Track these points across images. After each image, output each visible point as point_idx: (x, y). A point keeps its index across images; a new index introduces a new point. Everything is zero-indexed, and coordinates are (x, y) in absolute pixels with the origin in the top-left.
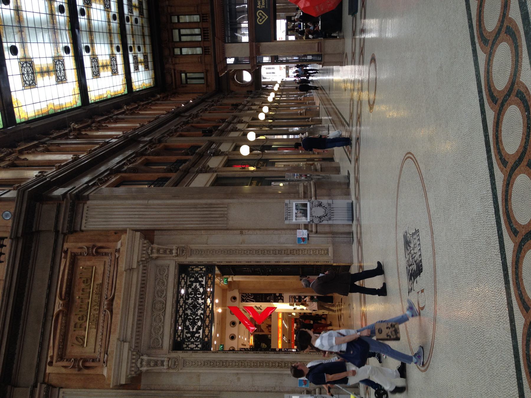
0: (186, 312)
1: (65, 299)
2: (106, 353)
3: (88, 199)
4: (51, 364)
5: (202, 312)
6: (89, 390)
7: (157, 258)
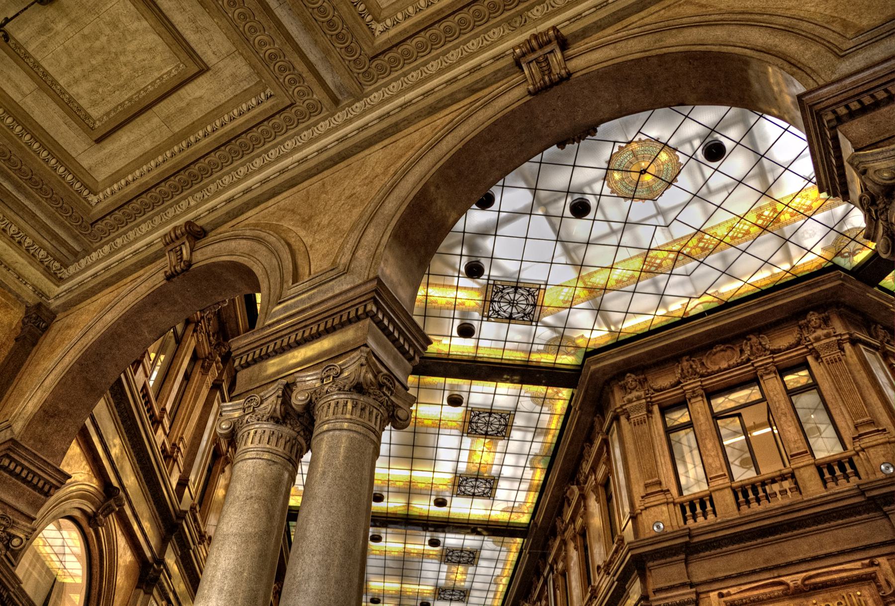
1: (805, 585)
4: (721, 595)
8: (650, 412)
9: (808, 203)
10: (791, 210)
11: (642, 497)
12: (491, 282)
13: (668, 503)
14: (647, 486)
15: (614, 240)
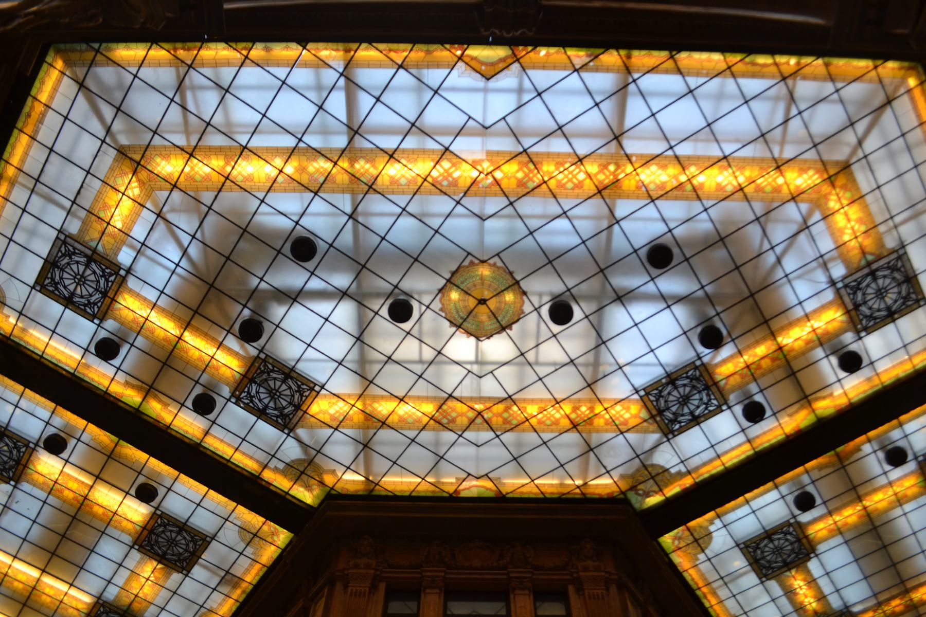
8: (374, 588)
9: (627, 416)
10: (607, 416)
12: (262, 356)
15: (418, 369)
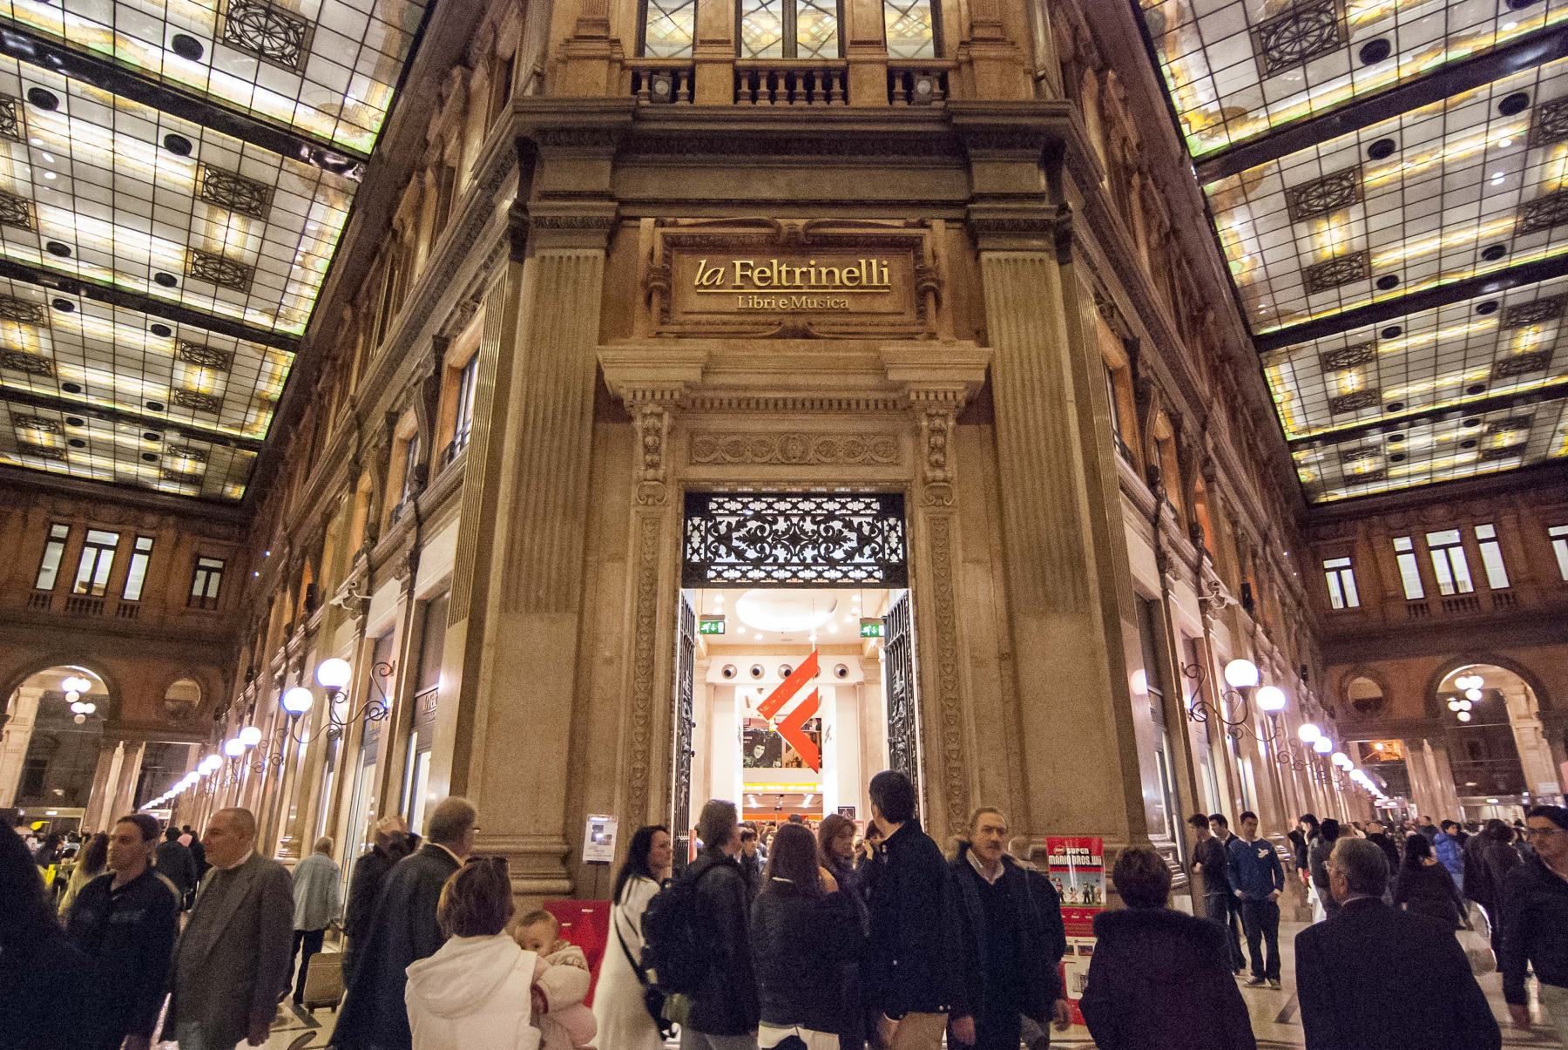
0: (781, 519)
2: (680, 336)
3: (1061, 264)
4: (660, 223)
5: (781, 560)
6: (598, 309)
7: (917, 432)
11: (568, 41)
13: (611, 61)
14: (580, 22)
